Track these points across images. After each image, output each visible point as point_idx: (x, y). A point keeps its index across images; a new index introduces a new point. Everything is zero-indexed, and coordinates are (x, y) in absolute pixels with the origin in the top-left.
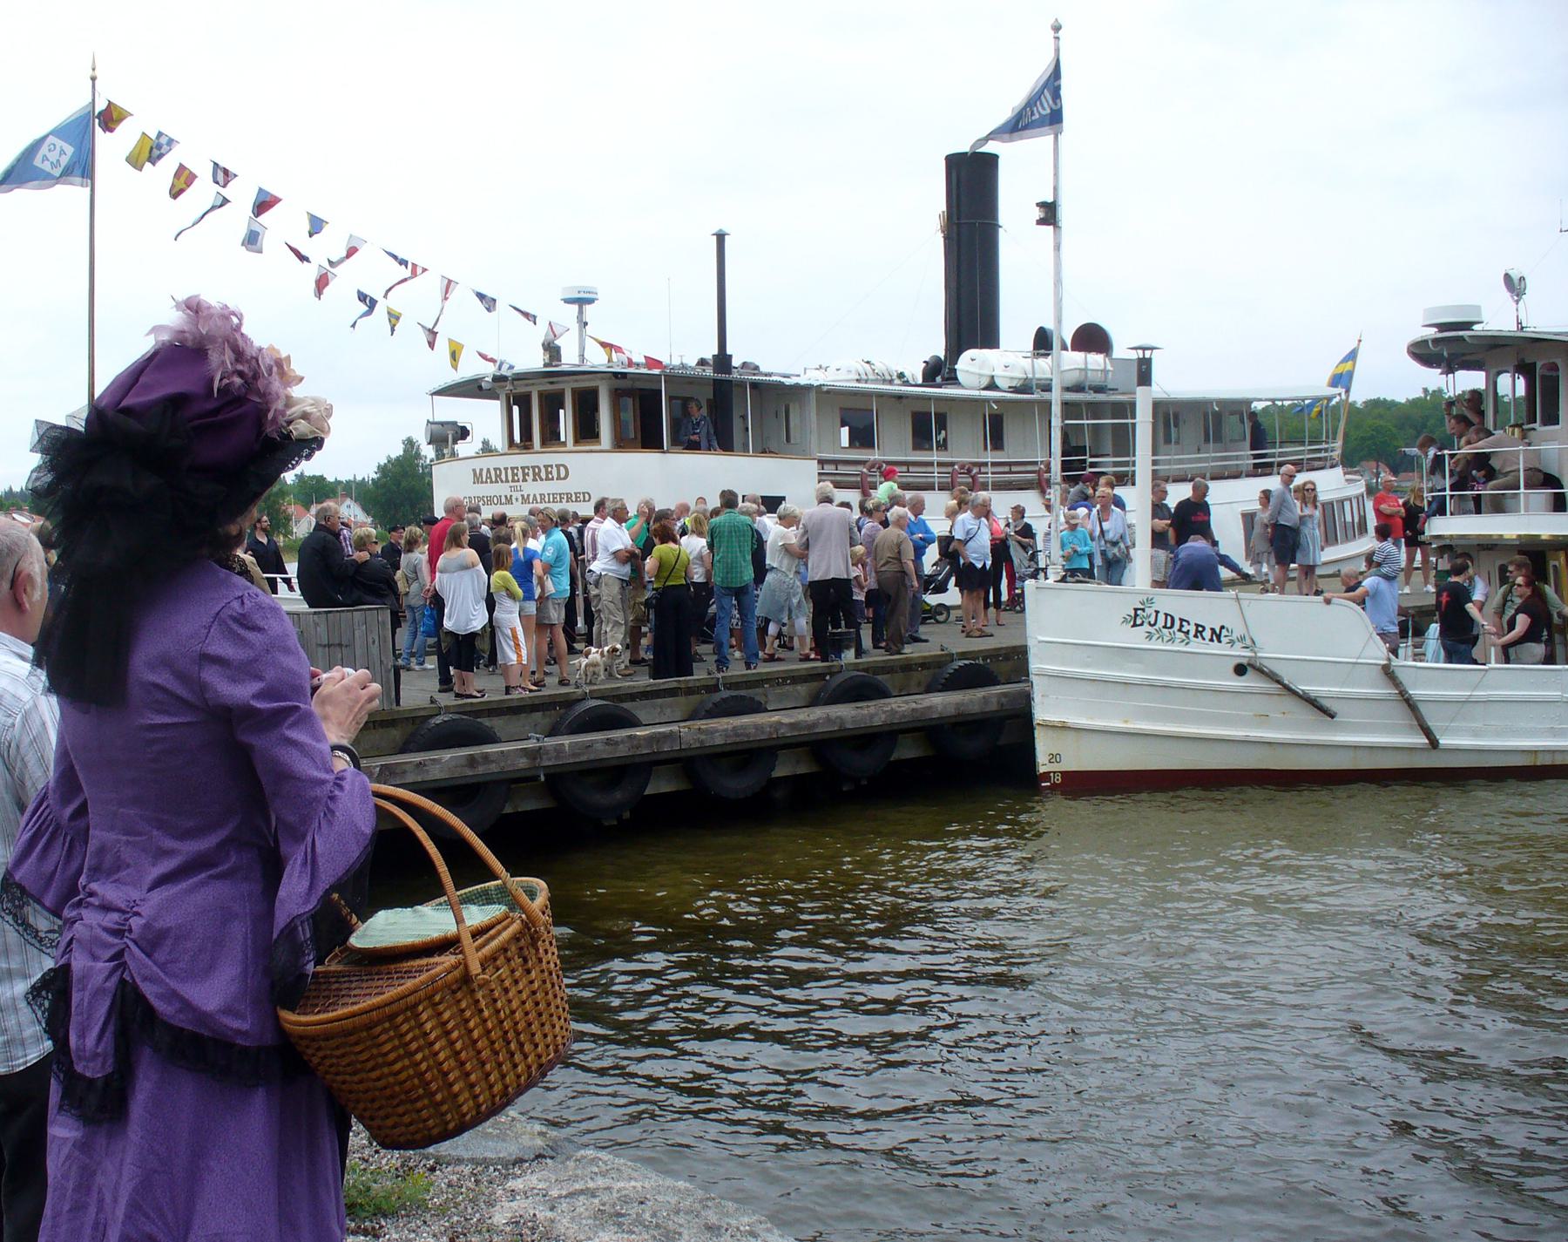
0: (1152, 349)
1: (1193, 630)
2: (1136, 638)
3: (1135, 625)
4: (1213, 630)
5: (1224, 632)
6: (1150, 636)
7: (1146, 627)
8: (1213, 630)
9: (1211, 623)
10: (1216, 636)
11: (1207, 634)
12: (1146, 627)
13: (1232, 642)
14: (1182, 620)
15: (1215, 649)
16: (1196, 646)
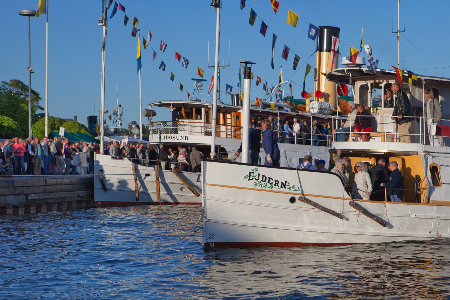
0: (252, 63)
1: (274, 182)
2: (251, 184)
3: (249, 180)
4: (282, 183)
5: (287, 184)
6: (256, 184)
7: (254, 181)
8: (282, 183)
9: (282, 180)
10: (284, 185)
11: (280, 184)
12: (254, 181)
13: (290, 188)
14: (269, 178)
15: (283, 190)
16: (275, 188)
